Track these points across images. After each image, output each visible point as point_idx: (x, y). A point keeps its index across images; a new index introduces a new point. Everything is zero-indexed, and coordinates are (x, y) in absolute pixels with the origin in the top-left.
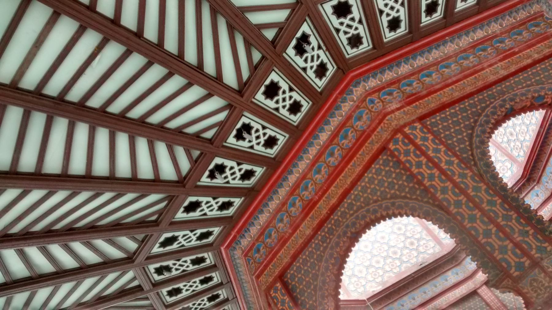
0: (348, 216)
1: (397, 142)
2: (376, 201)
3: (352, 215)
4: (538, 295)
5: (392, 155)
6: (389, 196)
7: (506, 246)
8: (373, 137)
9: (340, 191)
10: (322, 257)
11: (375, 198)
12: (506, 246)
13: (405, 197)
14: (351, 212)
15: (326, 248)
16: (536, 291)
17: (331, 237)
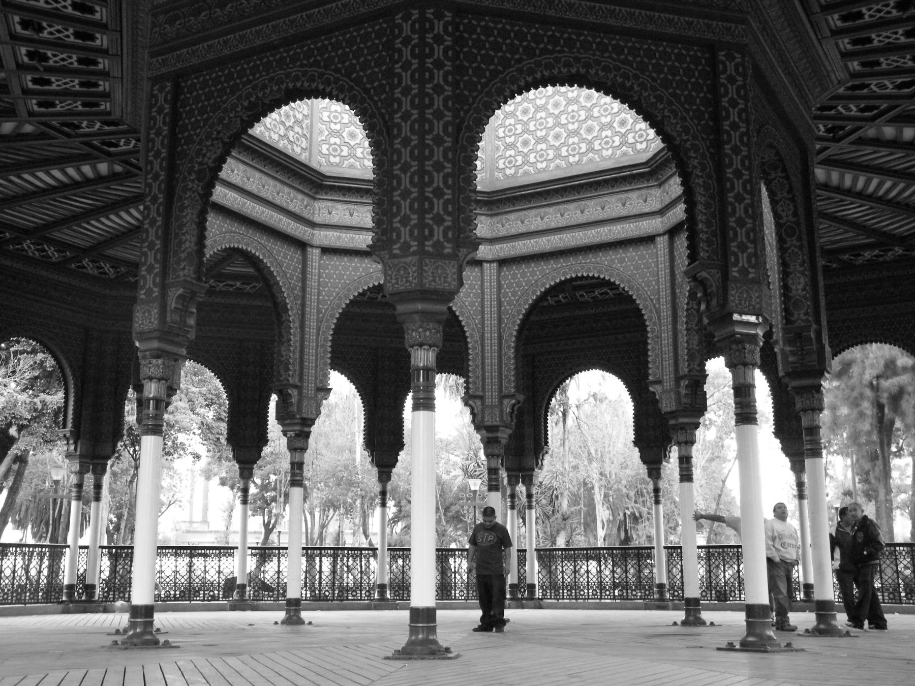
0: (607, 55)
1: (730, 57)
2: (654, 80)
3: (614, 60)
4: (740, 304)
5: (713, 62)
6: (671, 91)
7: (747, 248)
8: (714, 23)
9: (629, 24)
10: (534, 55)
11: (654, 75)
12: (747, 248)
13: (687, 111)
14: (615, 56)
15: (545, 51)
16: (740, 300)
17: (566, 49)
